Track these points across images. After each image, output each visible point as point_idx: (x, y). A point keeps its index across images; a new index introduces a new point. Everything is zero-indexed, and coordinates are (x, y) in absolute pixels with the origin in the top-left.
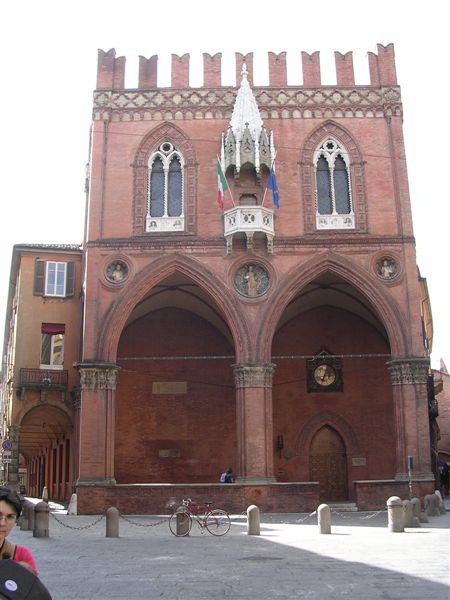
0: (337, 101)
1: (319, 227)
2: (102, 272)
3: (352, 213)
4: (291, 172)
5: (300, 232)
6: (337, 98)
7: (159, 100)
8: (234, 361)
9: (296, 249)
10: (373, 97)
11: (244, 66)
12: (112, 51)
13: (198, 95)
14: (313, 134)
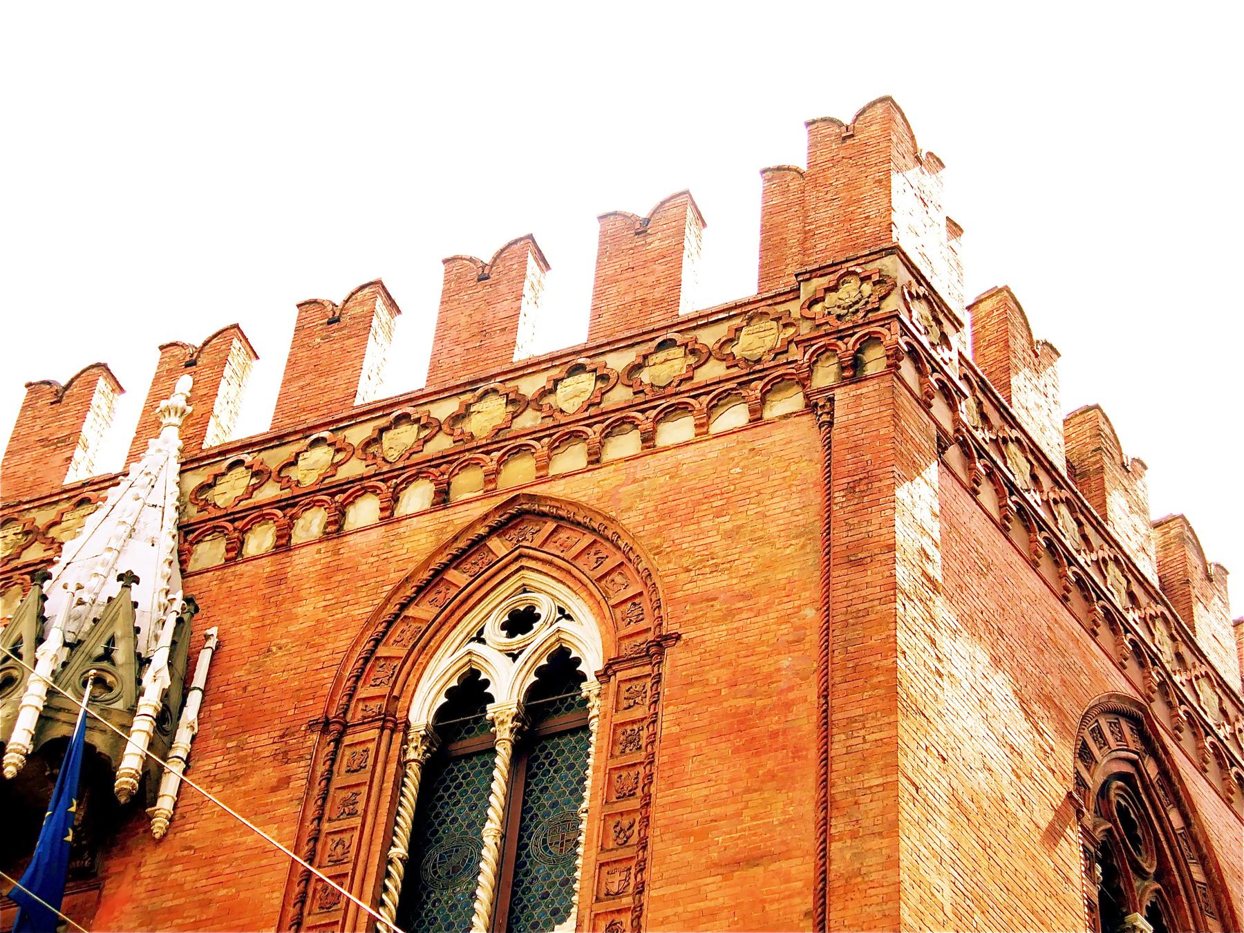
10: (757, 341)
11: (185, 383)
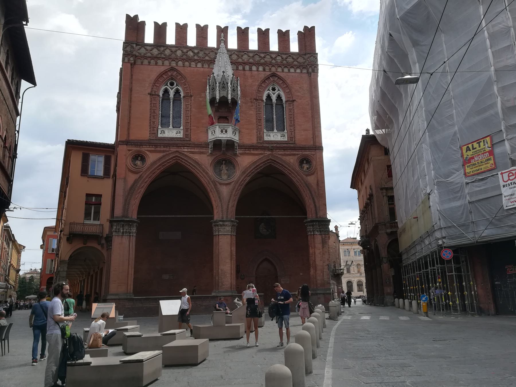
0: (279, 61)
1: (266, 138)
2: (129, 160)
3: (286, 131)
4: (250, 104)
5: (254, 141)
6: (279, 58)
7: (167, 52)
8: (212, 218)
9: (253, 152)
10: (301, 60)
11: (222, 34)
12: (136, 17)
13: (193, 52)
14: (264, 81)
